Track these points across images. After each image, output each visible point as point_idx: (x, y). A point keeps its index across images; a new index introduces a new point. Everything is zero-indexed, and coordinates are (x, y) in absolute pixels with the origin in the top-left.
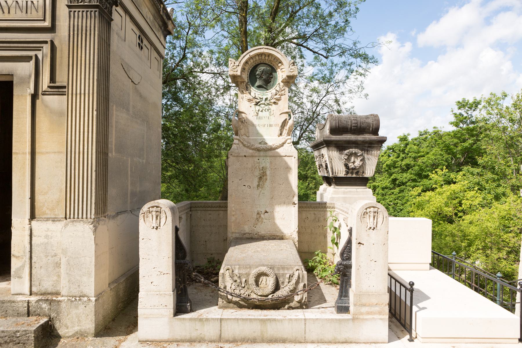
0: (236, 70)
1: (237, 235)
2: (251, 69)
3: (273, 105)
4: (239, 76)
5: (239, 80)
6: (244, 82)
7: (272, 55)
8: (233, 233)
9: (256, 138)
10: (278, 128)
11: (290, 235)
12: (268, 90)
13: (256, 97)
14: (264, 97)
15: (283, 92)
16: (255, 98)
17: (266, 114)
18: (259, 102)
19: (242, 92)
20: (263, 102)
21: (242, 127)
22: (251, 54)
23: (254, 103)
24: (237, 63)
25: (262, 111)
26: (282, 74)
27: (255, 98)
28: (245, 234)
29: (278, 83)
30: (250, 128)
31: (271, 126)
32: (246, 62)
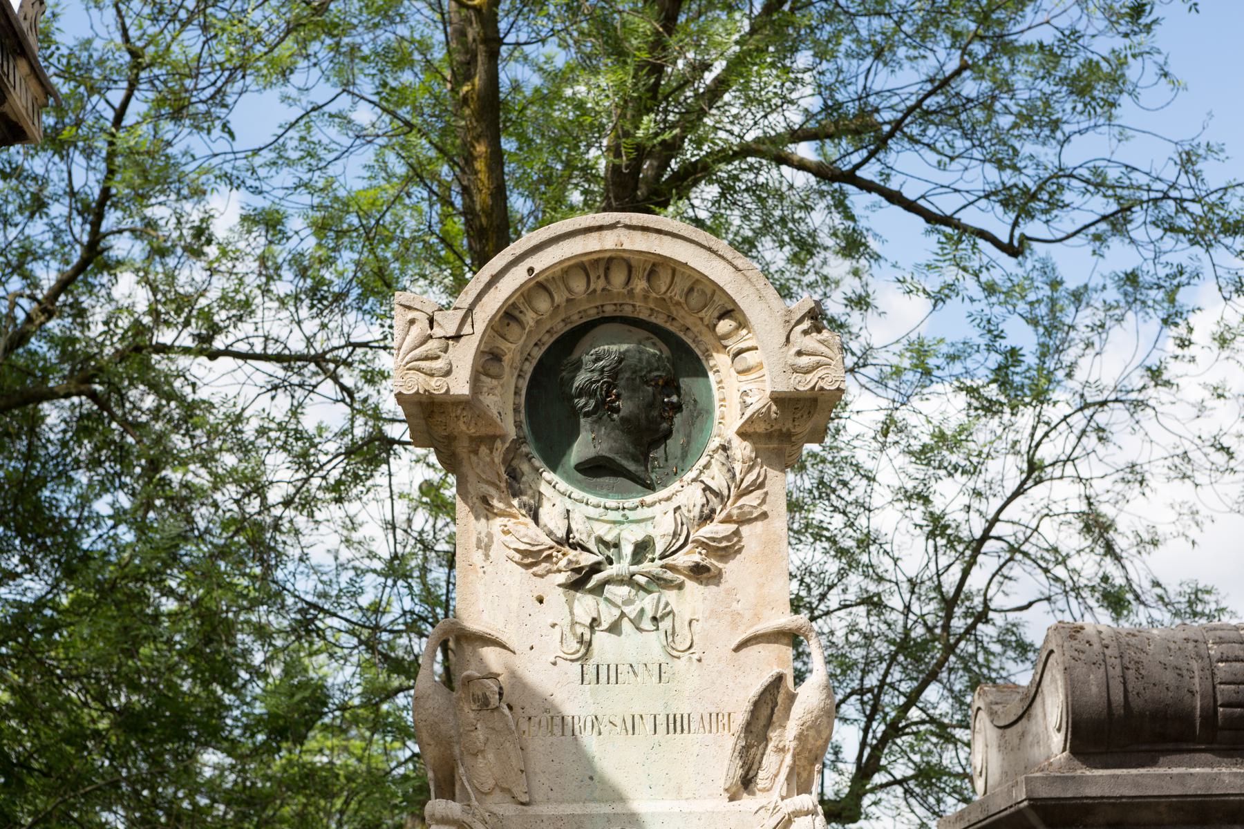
0: (439, 364)
2: (538, 353)
3: (690, 585)
4: (460, 402)
5: (464, 427)
6: (490, 440)
7: (674, 268)
9: (577, 809)
10: (728, 742)
12: (651, 488)
13: (577, 536)
14: (630, 536)
15: (752, 500)
16: (568, 541)
17: (649, 645)
18: (595, 568)
19: (484, 508)
20: (621, 567)
21: (480, 735)
22: (541, 262)
23: (562, 578)
24: (448, 324)
25: (614, 628)
26: (746, 382)
27: (568, 541)
29: (715, 443)
30: (539, 743)
31: (676, 724)
32: (509, 315)
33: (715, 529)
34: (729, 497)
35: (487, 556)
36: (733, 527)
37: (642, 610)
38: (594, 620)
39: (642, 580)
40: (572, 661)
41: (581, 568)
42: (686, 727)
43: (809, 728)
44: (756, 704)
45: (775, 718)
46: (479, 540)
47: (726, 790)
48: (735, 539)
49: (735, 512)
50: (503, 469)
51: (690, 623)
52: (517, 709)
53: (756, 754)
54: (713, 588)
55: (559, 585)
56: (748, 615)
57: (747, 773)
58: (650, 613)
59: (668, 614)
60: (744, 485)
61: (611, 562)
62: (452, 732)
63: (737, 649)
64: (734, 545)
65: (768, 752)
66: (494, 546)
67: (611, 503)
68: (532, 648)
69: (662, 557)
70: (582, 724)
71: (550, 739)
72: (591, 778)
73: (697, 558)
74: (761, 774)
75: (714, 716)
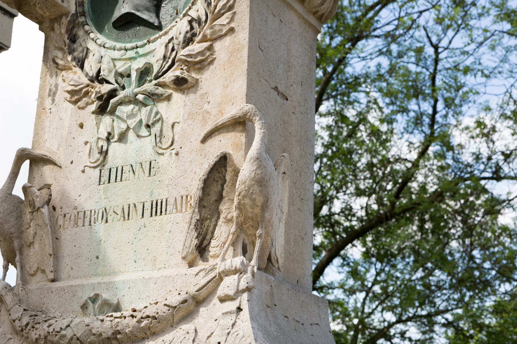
3: (177, 96)
15: (224, 20)
16: (98, 78)
18: (112, 94)
23: (93, 107)
27: (98, 78)
33: (196, 47)
34: (206, 21)
35: (53, 100)
36: (206, 44)
37: (141, 121)
38: (109, 134)
39: (140, 97)
40: (95, 167)
41: (102, 96)
42: (163, 210)
43: (244, 197)
44: (205, 181)
45: (224, 194)
46: (50, 90)
47: (184, 258)
48: (208, 54)
49: (208, 32)
50: (66, 37)
51: (173, 126)
52: (58, 210)
53: (209, 226)
54: (192, 96)
55: (93, 113)
56: (214, 112)
57: (201, 243)
58: (144, 122)
59: (158, 120)
60: (216, 11)
61: (123, 88)
62: (12, 230)
63: (204, 140)
64: (207, 58)
65: (220, 223)
66: (59, 92)
67: (129, 45)
68: (72, 163)
69: (156, 78)
70: (96, 216)
71: (76, 230)
72: (97, 258)
73: (178, 73)
74: (213, 243)
75: (184, 197)
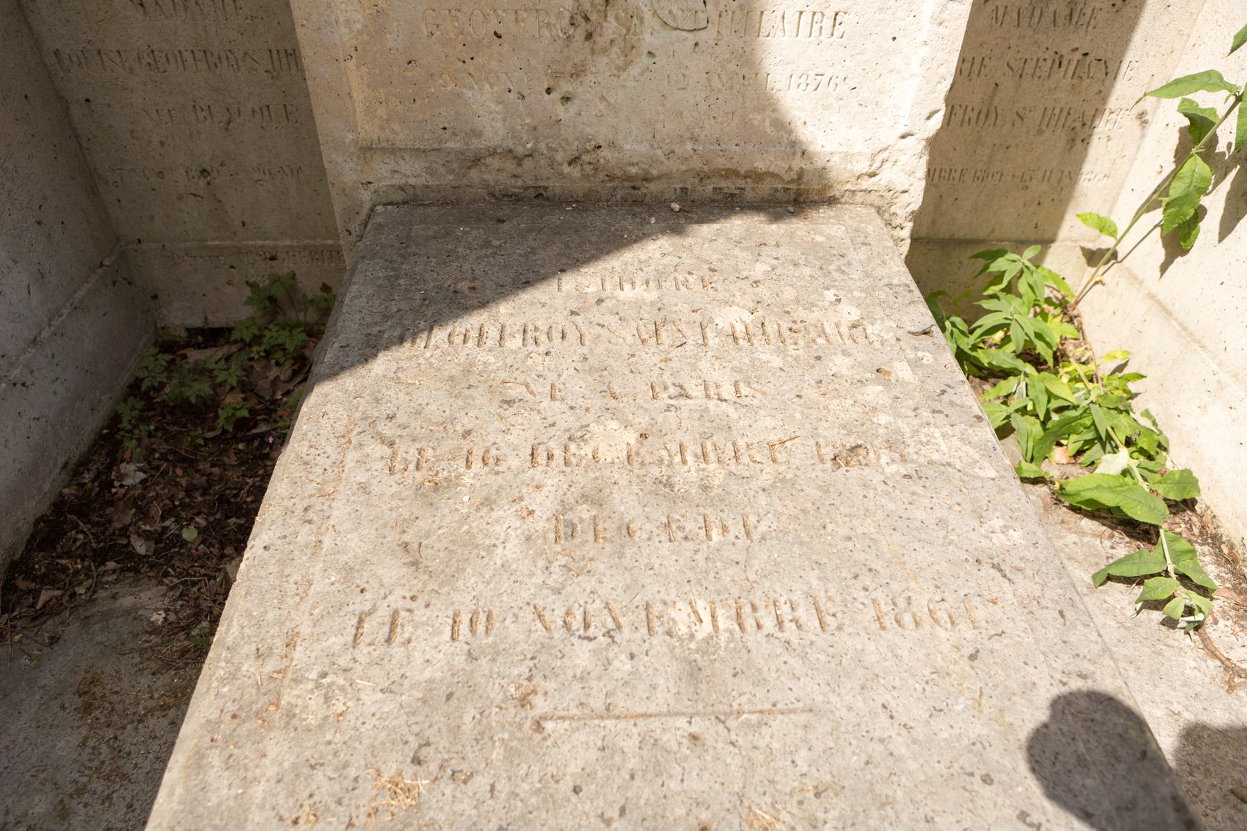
1: (413, 172)
8: (367, 150)
11: (863, 166)
28: (477, 160)
